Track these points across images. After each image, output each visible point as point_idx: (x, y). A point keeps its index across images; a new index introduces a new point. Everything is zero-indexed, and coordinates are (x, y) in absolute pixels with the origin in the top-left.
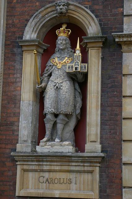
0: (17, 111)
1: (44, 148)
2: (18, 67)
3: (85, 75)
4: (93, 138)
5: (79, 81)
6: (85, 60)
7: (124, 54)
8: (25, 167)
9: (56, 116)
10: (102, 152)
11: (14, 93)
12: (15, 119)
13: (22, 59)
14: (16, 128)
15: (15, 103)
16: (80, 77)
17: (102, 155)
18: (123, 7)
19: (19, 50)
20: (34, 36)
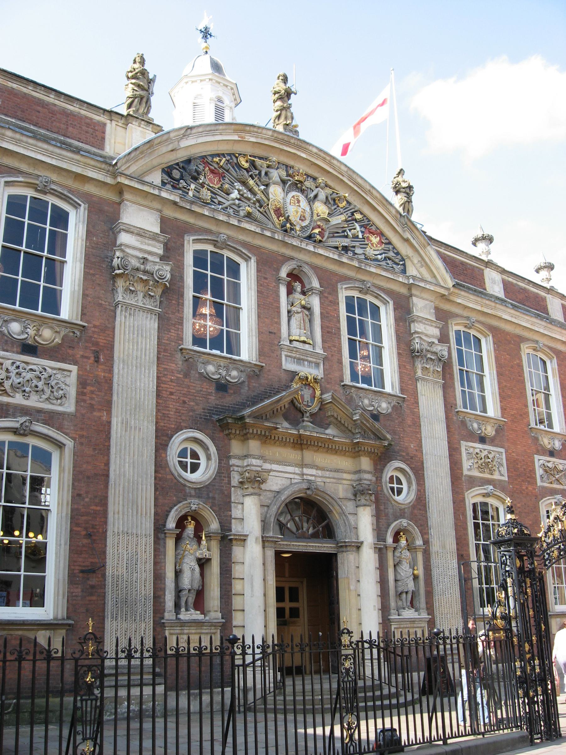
0: (163, 586)
1: (184, 616)
2: (162, 549)
3: (209, 560)
4: (216, 609)
5: (203, 563)
6: (208, 550)
7: (234, 547)
8: (172, 631)
9: (189, 590)
10: (222, 618)
11: (160, 572)
12: (161, 593)
13: (165, 543)
14: (162, 600)
15: (161, 580)
16: (204, 561)
17: (224, 621)
18: (231, 511)
19: (163, 535)
20: (174, 525)
